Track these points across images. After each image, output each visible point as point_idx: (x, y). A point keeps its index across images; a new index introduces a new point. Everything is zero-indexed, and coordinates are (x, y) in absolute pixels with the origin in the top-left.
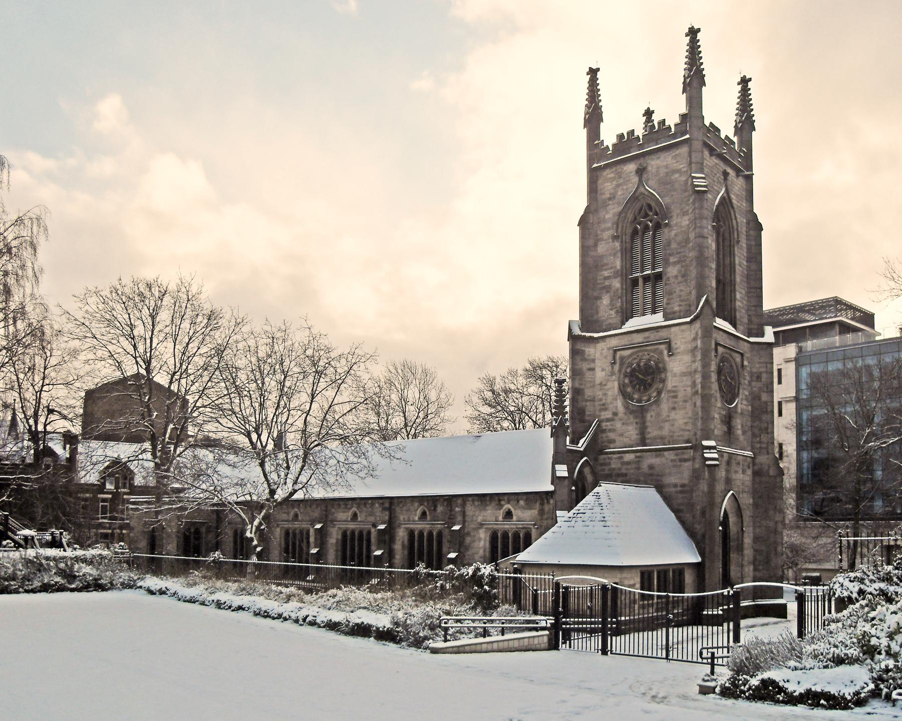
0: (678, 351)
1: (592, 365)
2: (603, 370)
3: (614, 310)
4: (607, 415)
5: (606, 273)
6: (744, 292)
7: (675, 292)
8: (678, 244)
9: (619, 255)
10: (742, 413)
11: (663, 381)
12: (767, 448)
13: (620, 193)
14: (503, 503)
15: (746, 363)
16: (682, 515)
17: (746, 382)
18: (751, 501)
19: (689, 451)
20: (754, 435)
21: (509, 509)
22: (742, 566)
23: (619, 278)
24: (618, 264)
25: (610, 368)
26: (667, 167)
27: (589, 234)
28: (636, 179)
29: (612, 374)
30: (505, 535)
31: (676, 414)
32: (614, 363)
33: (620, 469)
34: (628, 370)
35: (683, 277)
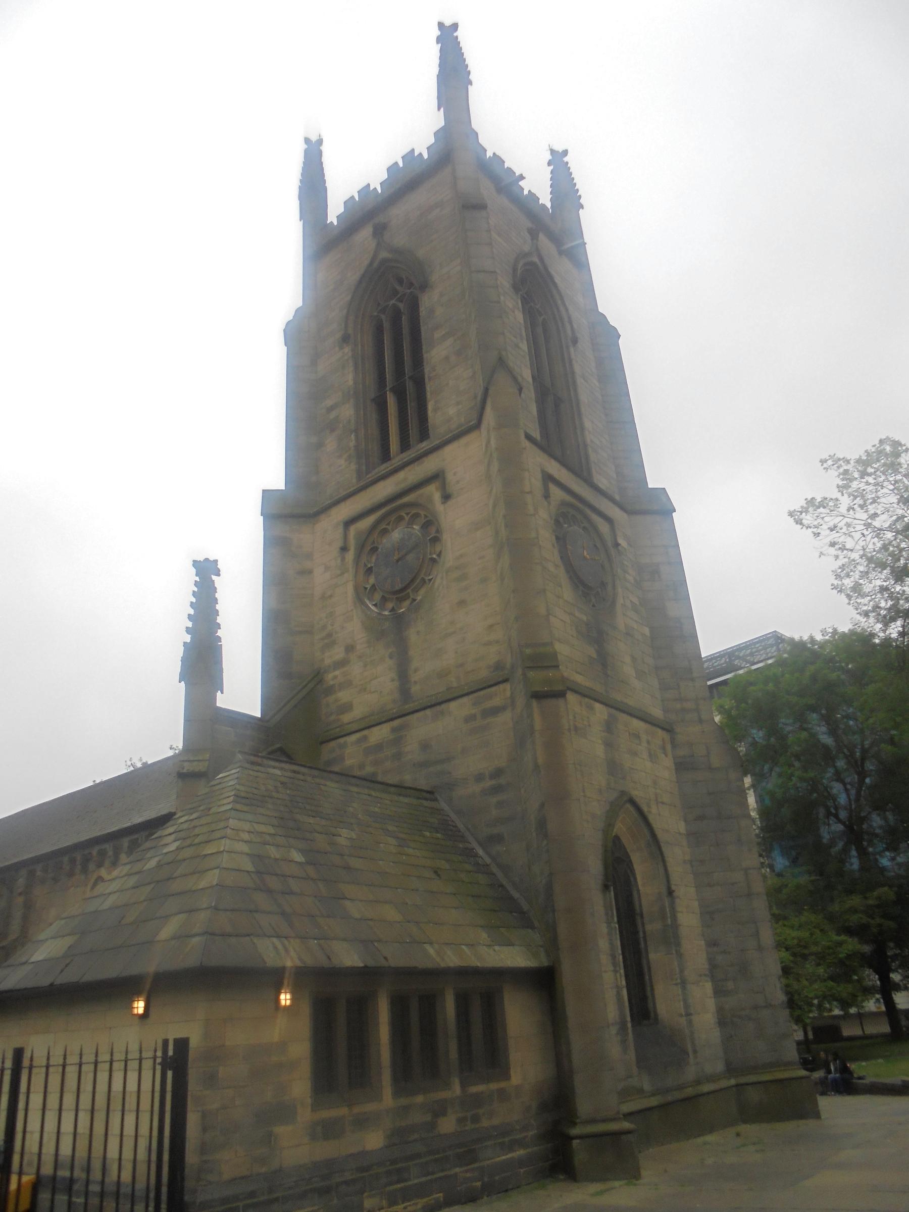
2: (327, 568)
4: (338, 653)
10: (628, 634)
18: (682, 827)
19: (501, 686)
22: (683, 983)
25: (339, 561)
33: (362, 766)
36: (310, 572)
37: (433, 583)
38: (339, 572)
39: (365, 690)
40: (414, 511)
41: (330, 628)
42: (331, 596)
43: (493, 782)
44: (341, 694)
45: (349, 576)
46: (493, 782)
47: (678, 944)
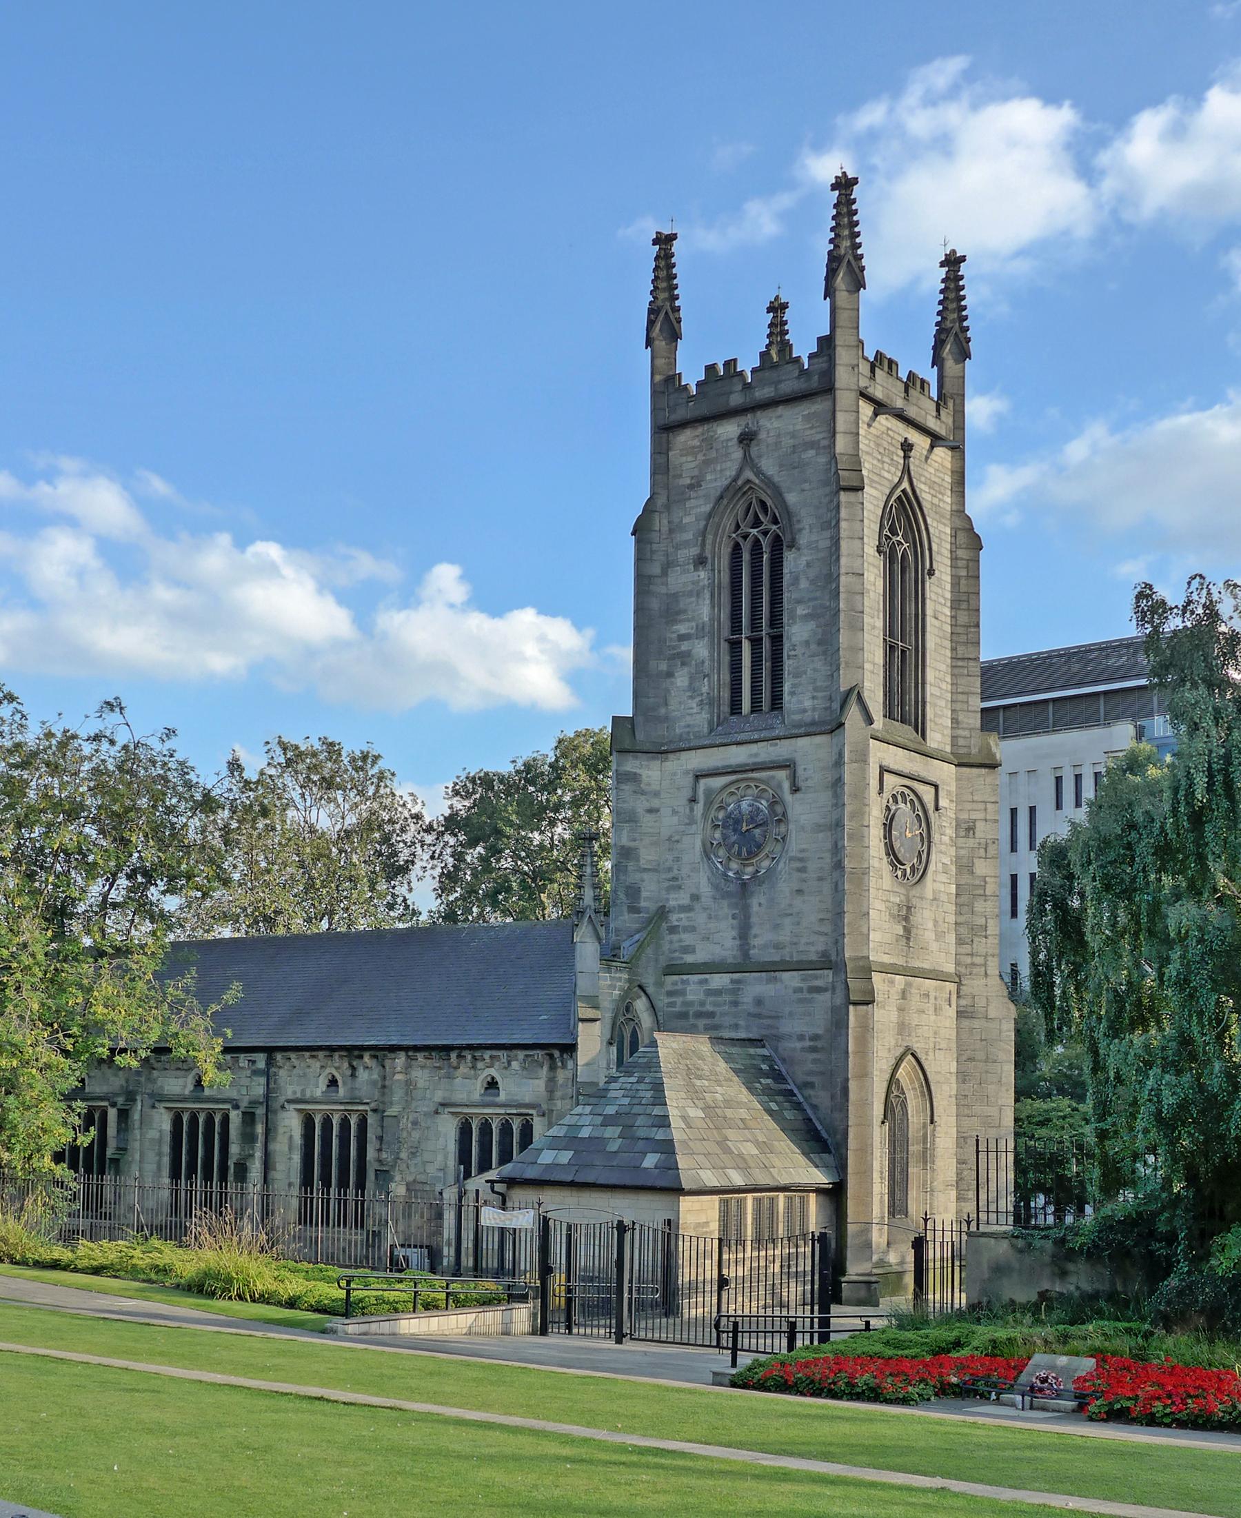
0: (809, 783)
1: (655, 803)
2: (675, 812)
4: (683, 898)
5: (683, 628)
6: (943, 667)
8: (813, 582)
9: (707, 595)
10: (935, 899)
12: (985, 965)
13: (709, 477)
14: (480, 1065)
15: (942, 803)
16: (811, 1092)
17: (946, 839)
18: (953, 1067)
19: (826, 972)
20: (960, 942)
21: (493, 1078)
23: (706, 639)
24: (704, 610)
26: (793, 435)
27: (652, 552)
28: (738, 454)
29: (692, 821)
31: (804, 902)
32: (693, 800)
33: (702, 1004)
34: (721, 815)
35: (819, 643)
36: (658, 811)
37: (778, 863)
38: (687, 821)
41: (676, 872)
42: (678, 841)
43: (812, 1044)
44: (684, 936)
45: (698, 828)
46: (812, 1044)
47: (933, 1162)
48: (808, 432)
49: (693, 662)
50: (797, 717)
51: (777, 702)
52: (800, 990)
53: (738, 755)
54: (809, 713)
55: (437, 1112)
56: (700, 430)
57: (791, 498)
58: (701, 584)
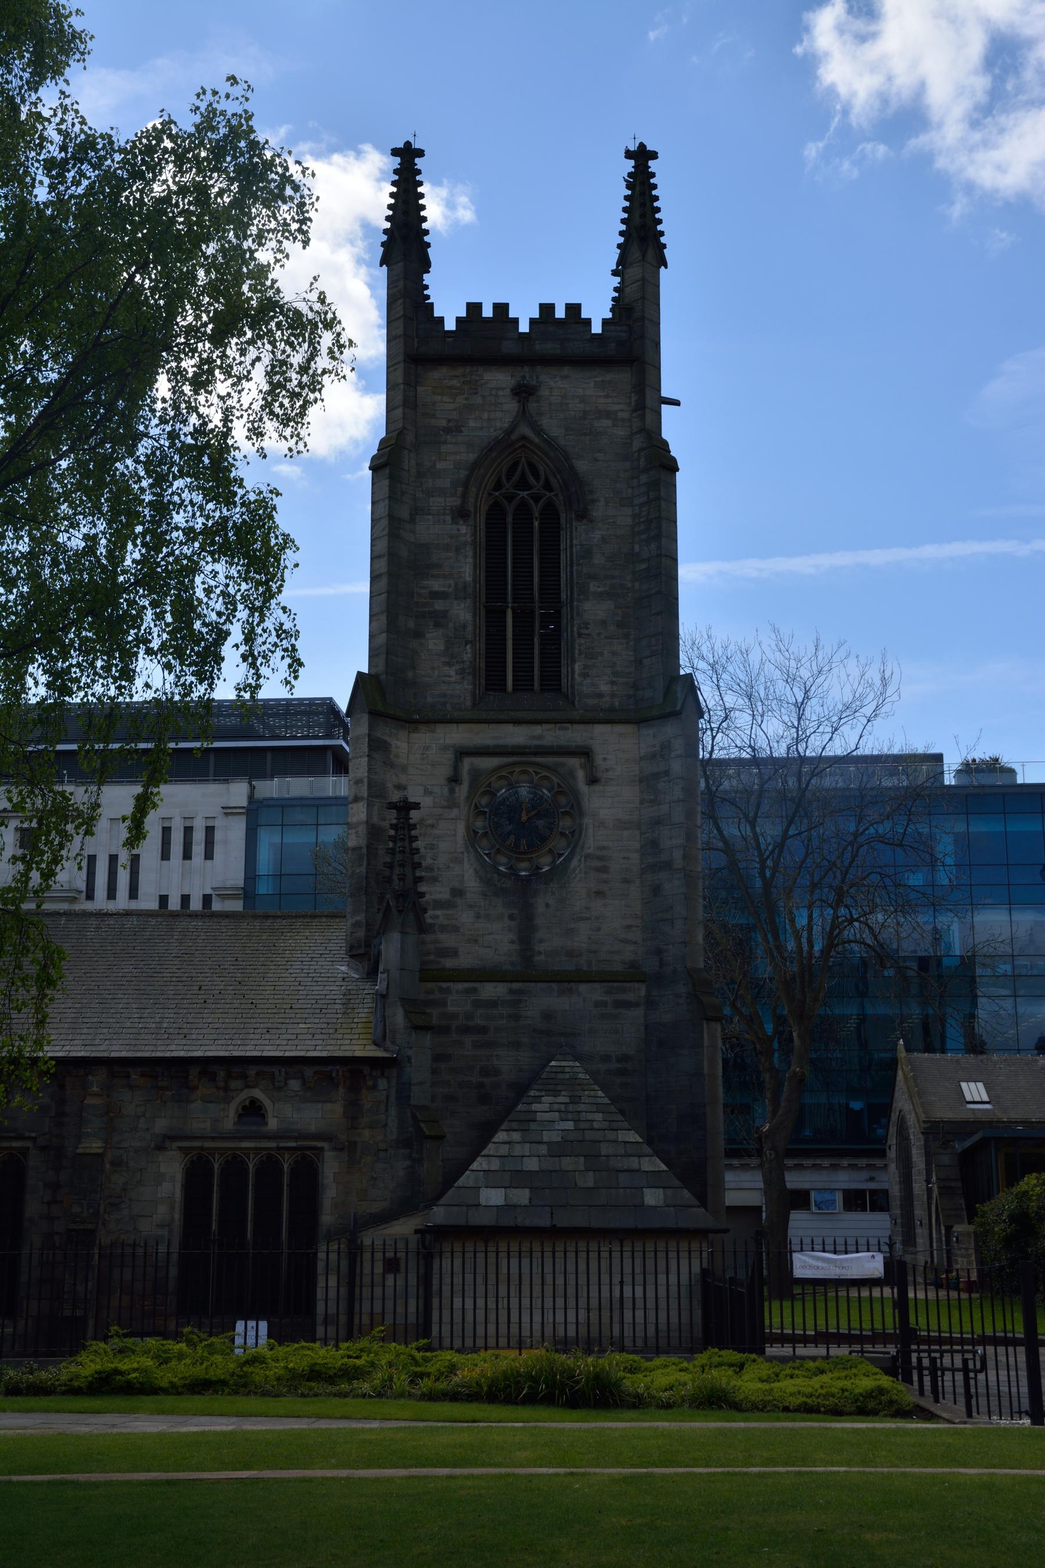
3: (457, 667)
5: (436, 585)
7: (601, 654)
11: (574, 837)
13: (472, 424)
14: (234, 1084)
19: (636, 985)
23: (469, 601)
25: (446, 791)
28: (511, 406)
29: (452, 804)
30: (235, 1165)
38: (445, 803)
39: (476, 941)
40: (544, 773)
42: (432, 826)
48: (602, 400)
49: (451, 625)
50: (591, 702)
51: (552, 681)
52: (604, 1004)
53: (516, 735)
54: (607, 699)
55: (160, 1148)
56: (460, 371)
57: (582, 466)
58: (463, 539)
